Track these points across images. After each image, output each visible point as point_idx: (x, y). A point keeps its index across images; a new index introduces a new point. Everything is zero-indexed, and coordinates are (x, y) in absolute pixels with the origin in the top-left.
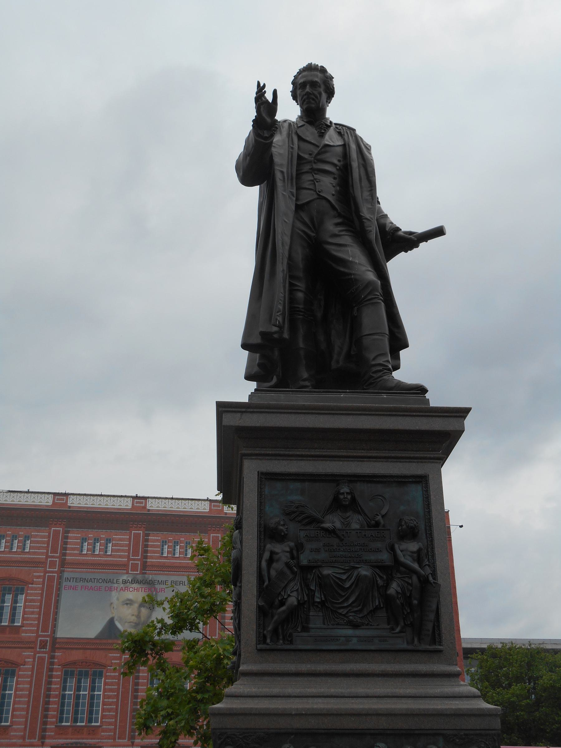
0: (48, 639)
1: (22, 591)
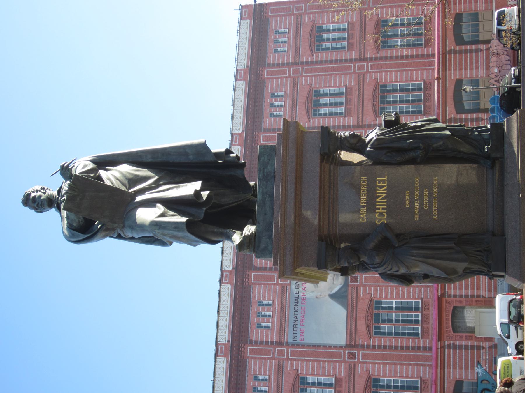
0: (347, 352)
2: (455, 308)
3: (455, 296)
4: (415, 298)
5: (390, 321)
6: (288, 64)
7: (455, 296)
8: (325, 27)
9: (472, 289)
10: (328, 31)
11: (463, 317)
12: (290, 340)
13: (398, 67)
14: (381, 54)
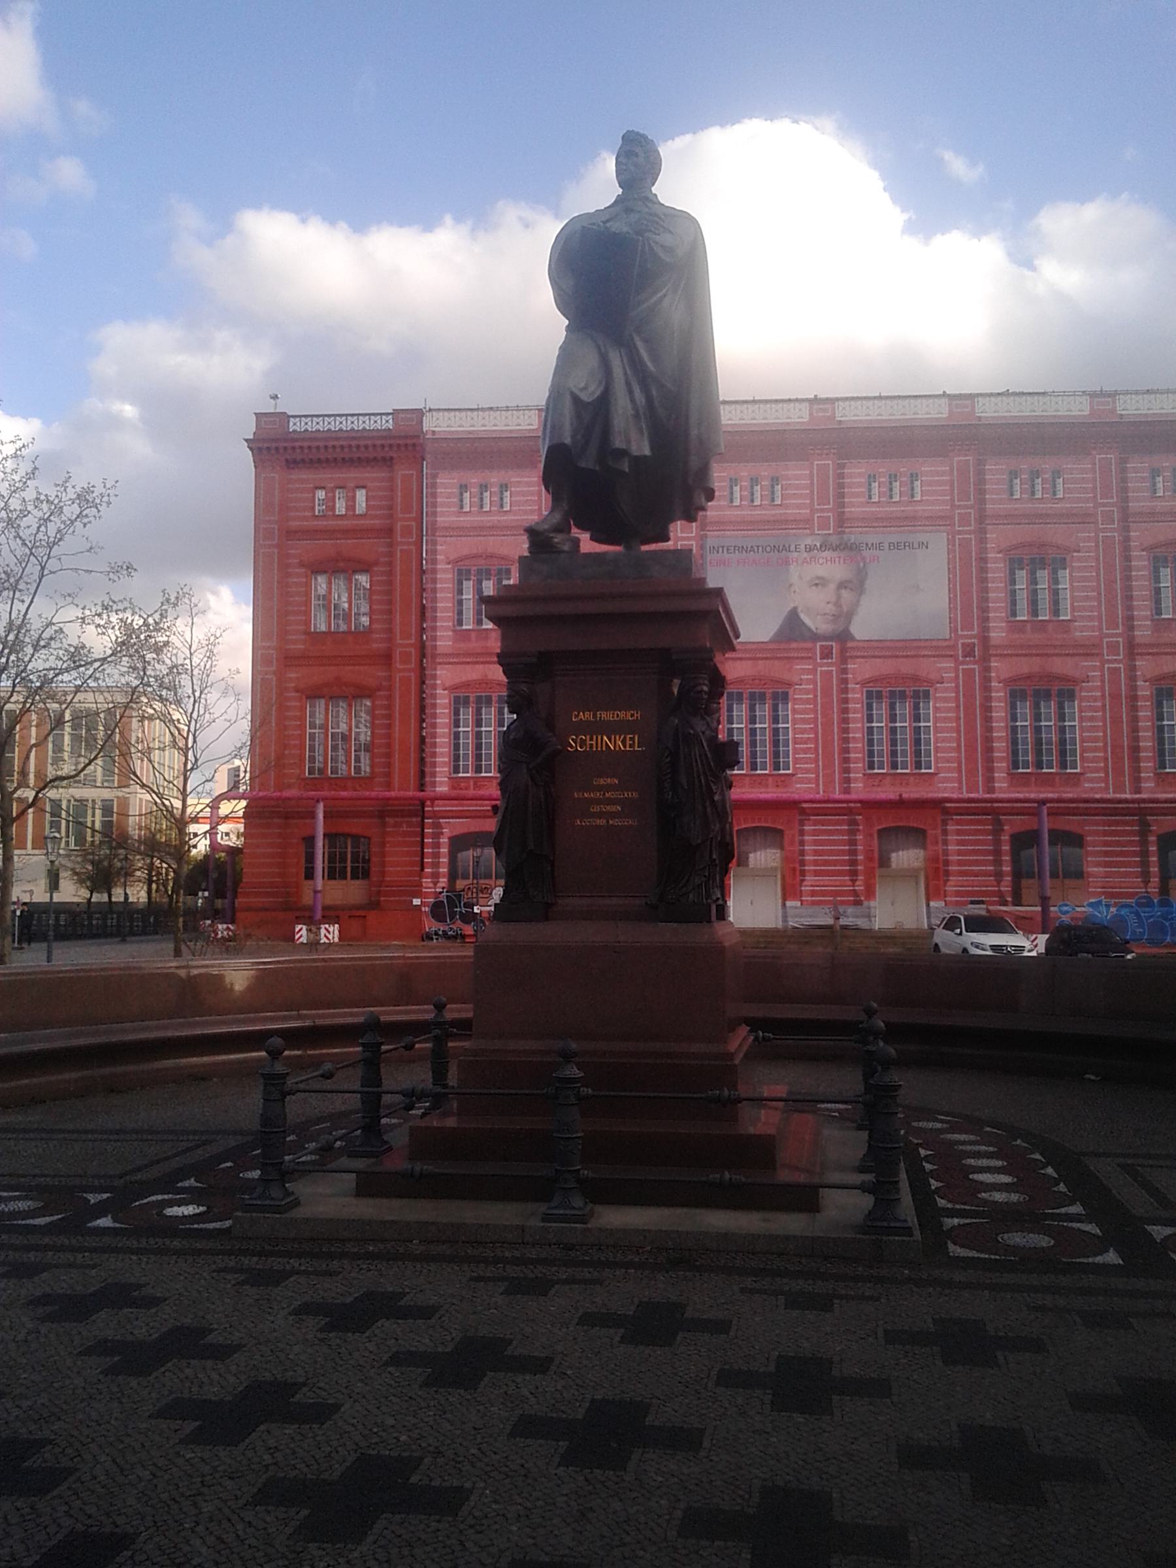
1: (1063, 564)
2: (781, 832)
3: (802, 833)
4: (795, 763)
5: (753, 720)
7: (802, 833)
9: (816, 863)
11: (770, 846)
12: (710, 542)
13: (1112, 722)
14: (853, 689)
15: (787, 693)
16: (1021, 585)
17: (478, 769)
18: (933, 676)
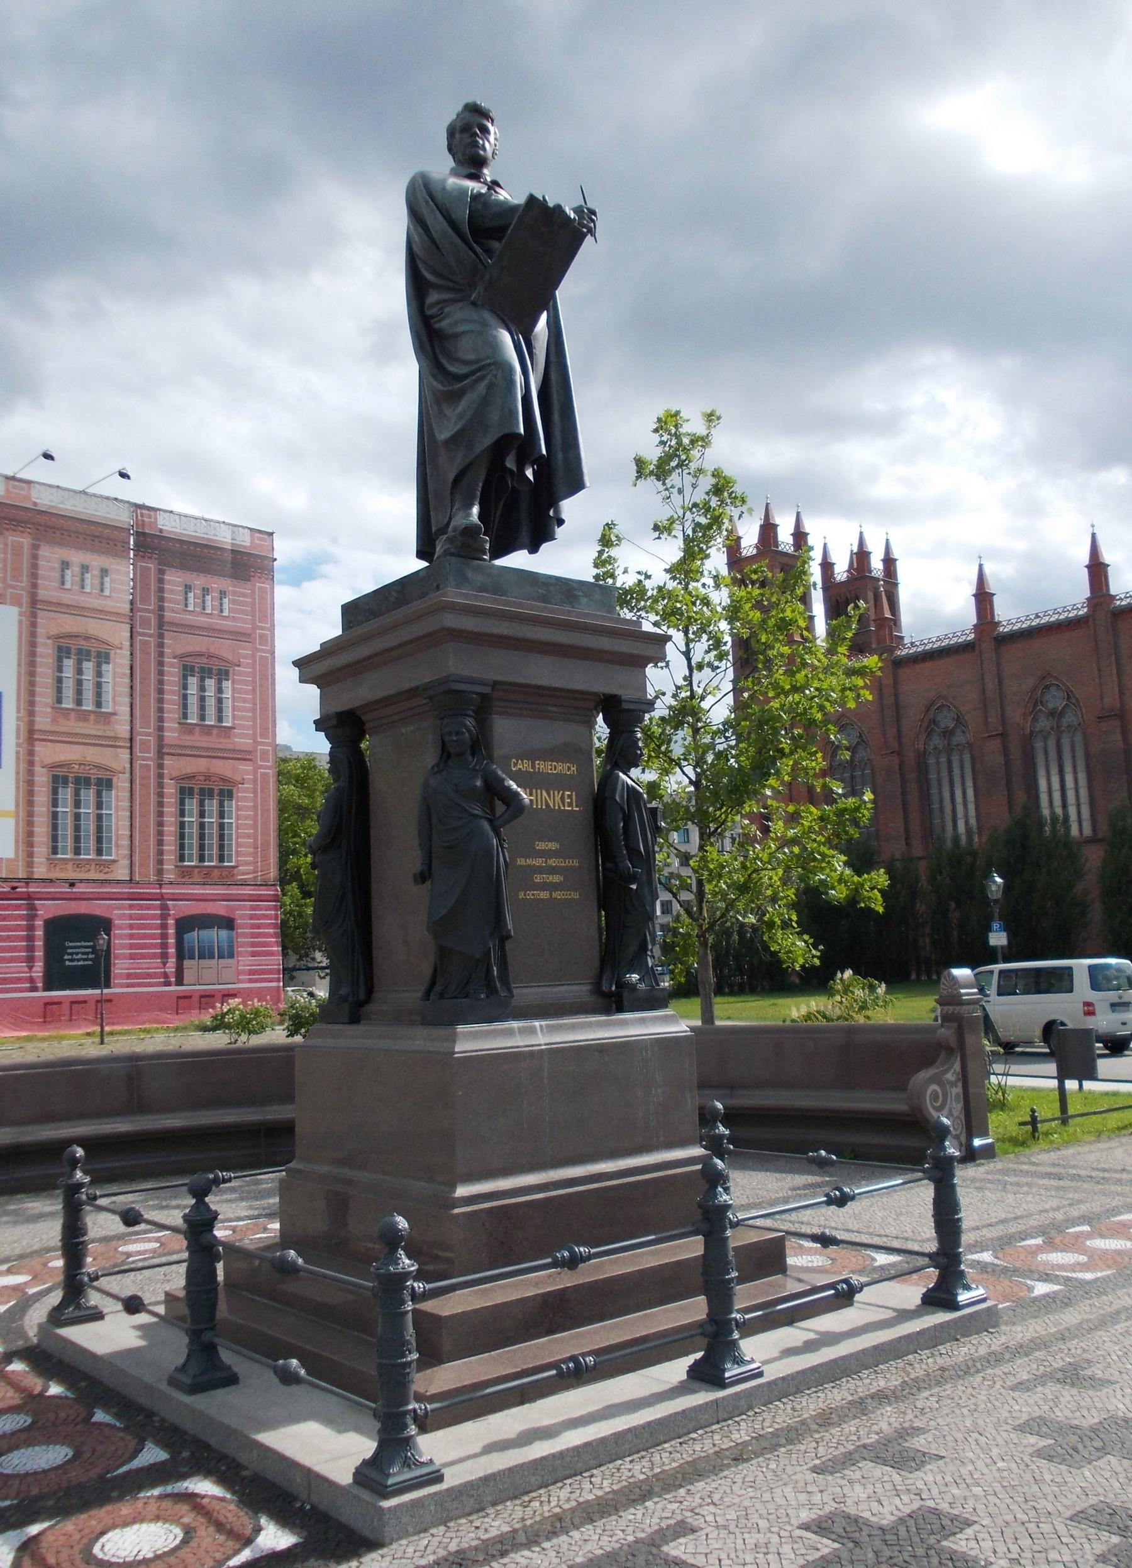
6: (161, 608)
8: (227, 685)
10: (220, 690)
15: (111, 780)
16: (193, 690)
17: (202, 858)
18: (237, 778)
